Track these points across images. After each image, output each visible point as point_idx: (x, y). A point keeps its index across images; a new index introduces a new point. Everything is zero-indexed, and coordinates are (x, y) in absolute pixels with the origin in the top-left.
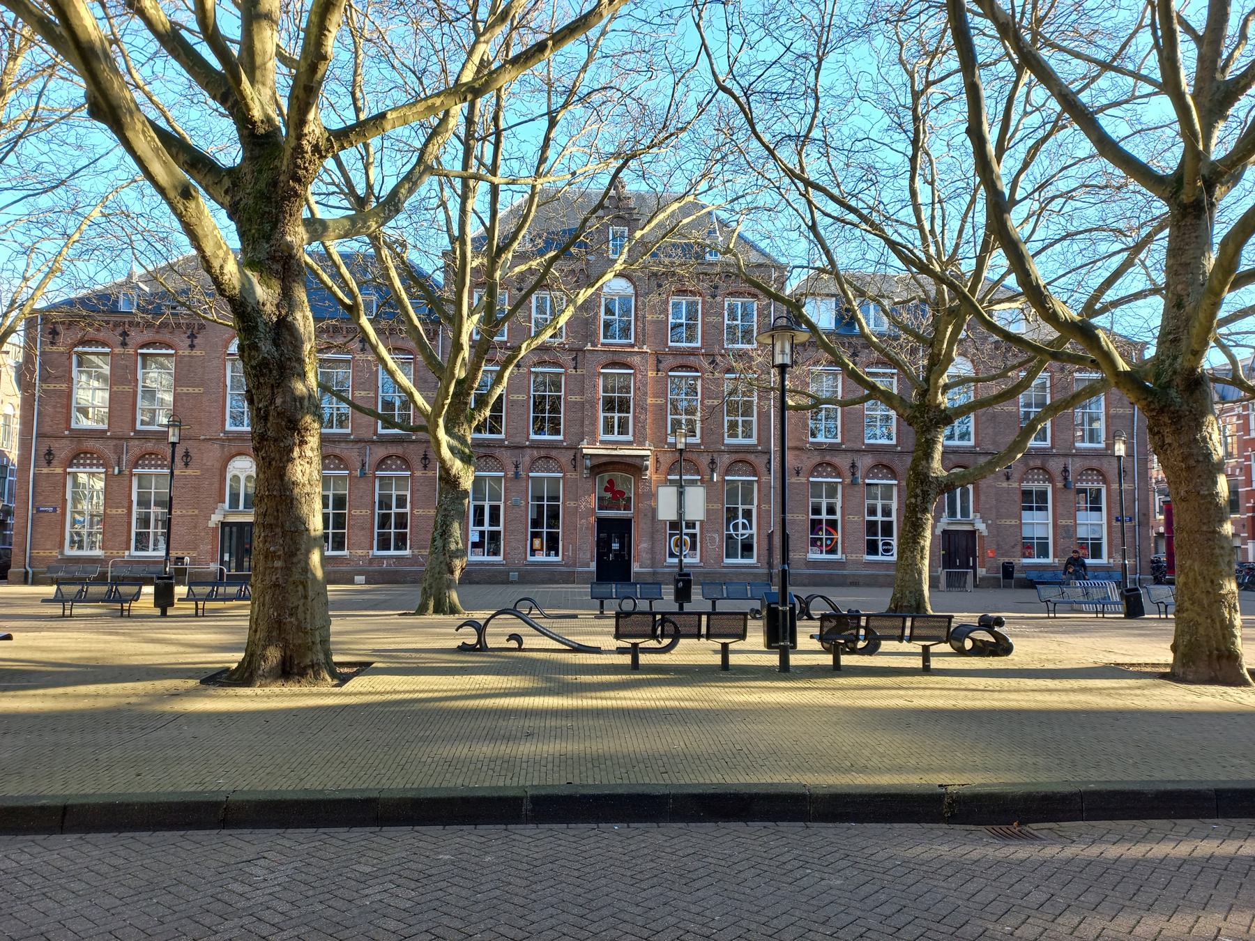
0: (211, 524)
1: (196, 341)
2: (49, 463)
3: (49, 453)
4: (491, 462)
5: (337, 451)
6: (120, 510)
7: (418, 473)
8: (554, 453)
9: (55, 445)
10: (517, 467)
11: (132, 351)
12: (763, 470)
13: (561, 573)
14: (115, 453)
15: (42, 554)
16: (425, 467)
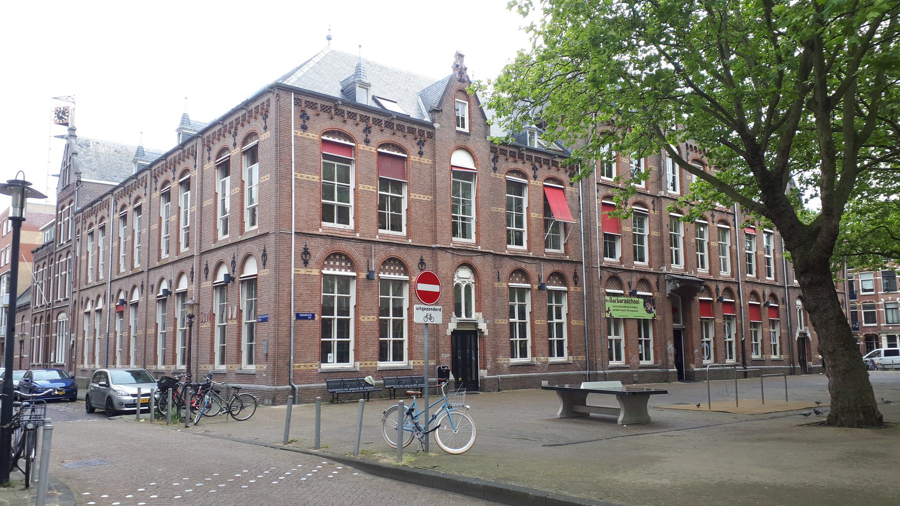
0: (449, 333)
1: (424, 149)
2: (306, 263)
3: (306, 252)
4: (614, 283)
5: (523, 265)
6: (371, 317)
7: (572, 289)
8: (647, 277)
9: (312, 243)
10: (630, 287)
11: (373, 150)
12: (736, 294)
13: (658, 373)
14: (365, 256)
15: (302, 368)
16: (576, 284)
